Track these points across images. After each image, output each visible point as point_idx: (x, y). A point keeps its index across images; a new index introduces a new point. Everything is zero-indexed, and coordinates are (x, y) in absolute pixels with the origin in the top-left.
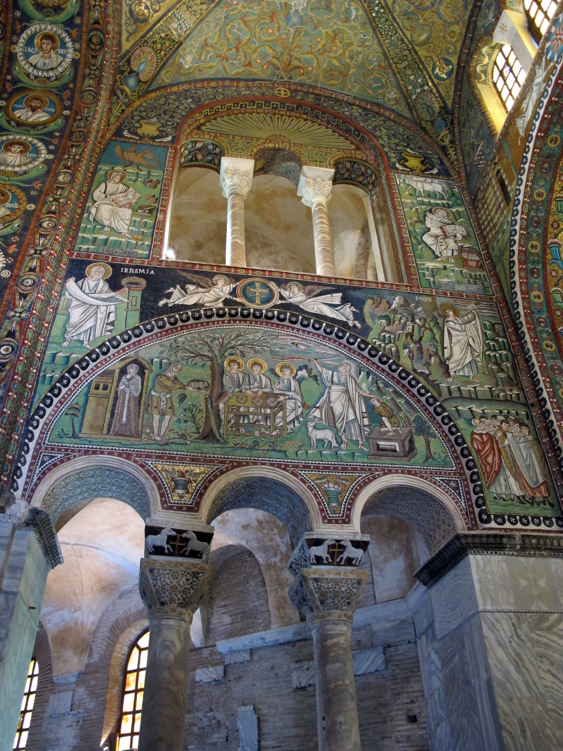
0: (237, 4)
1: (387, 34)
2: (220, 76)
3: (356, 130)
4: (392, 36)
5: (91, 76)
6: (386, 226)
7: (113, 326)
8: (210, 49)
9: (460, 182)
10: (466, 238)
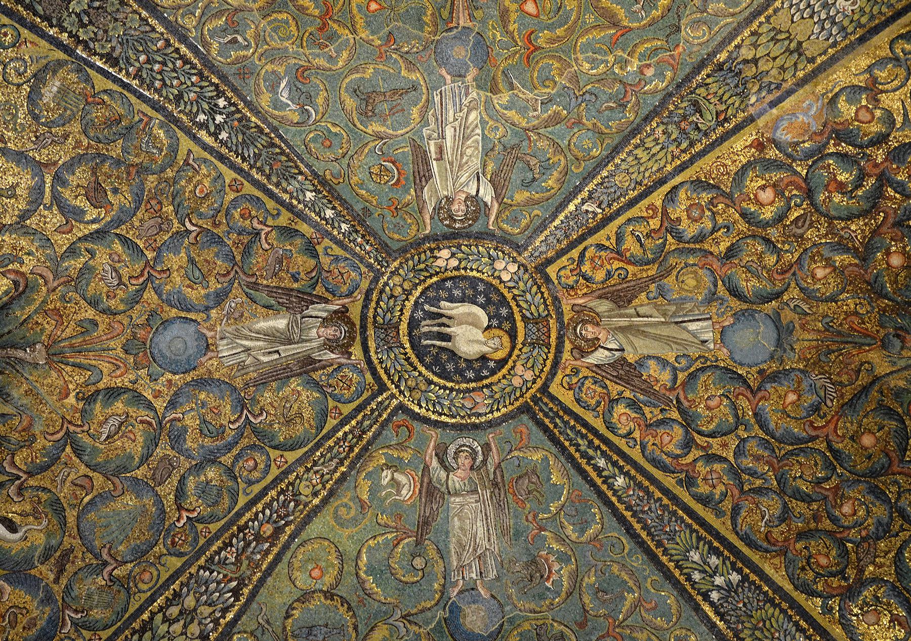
1: (164, 64)
4: (148, 61)
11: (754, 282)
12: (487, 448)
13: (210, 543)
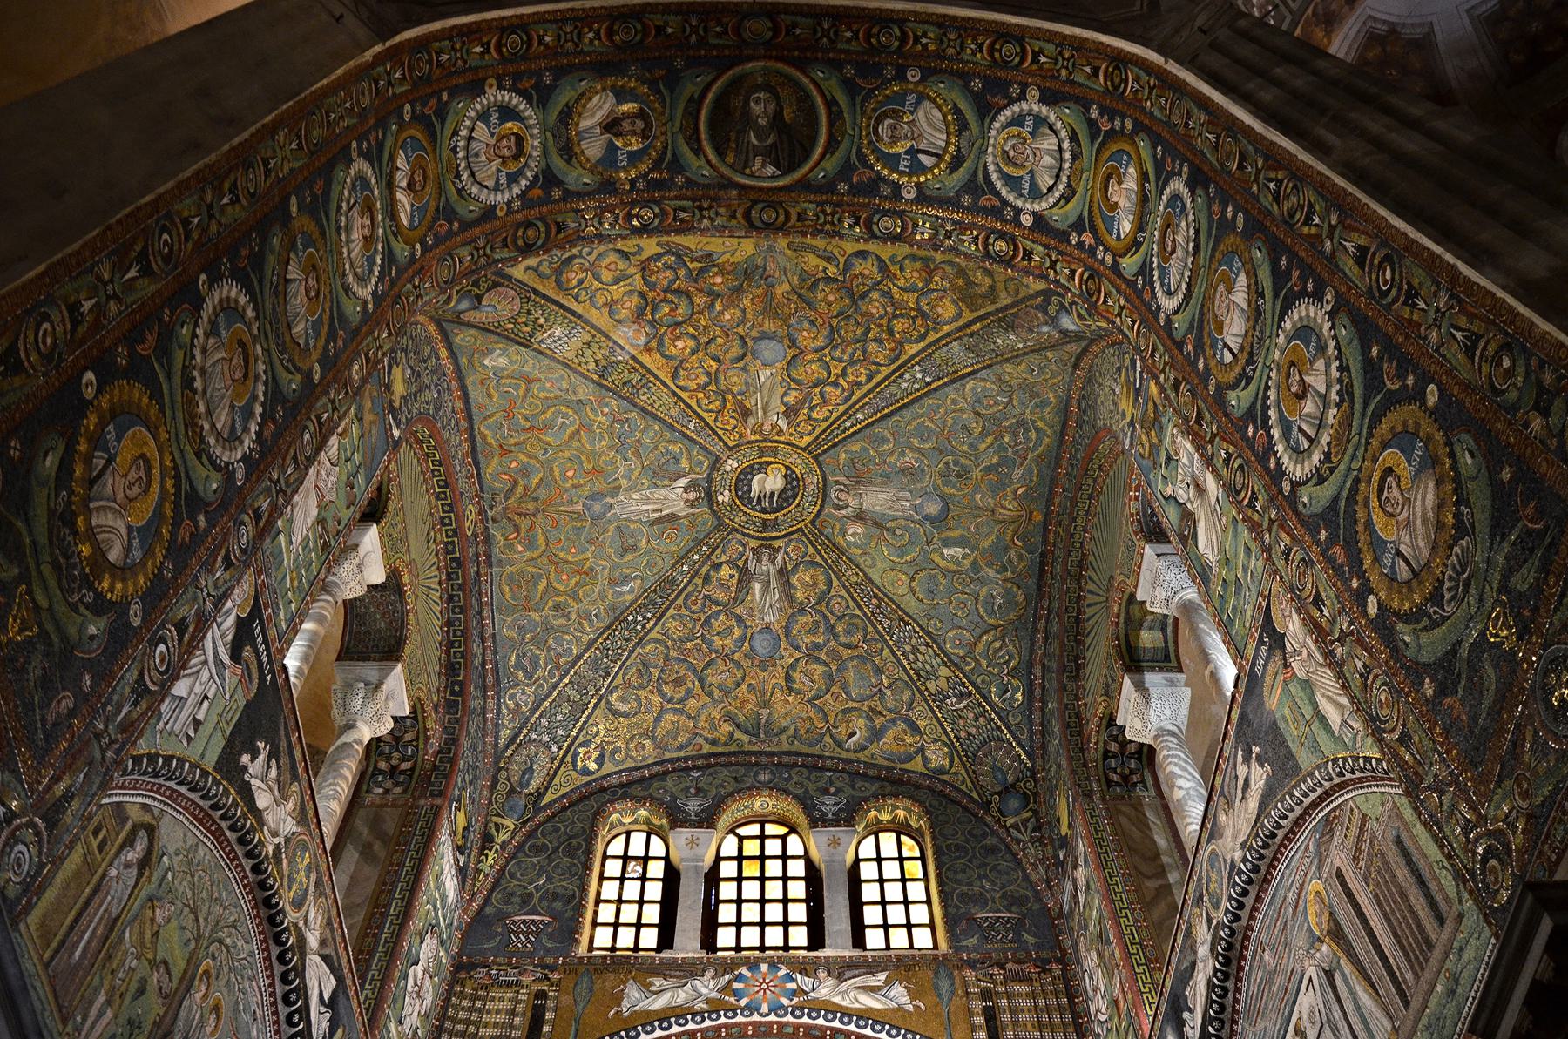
0: (603, 415)
2: (475, 410)
3: (460, 684)
5: (475, 253)
6: (372, 873)
7: (196, 731)
8: (523, 387)
9: (465, 911)
10: (427, 1015)
11: (734, 349)
12: (837, 482)
13: (878, 632)
